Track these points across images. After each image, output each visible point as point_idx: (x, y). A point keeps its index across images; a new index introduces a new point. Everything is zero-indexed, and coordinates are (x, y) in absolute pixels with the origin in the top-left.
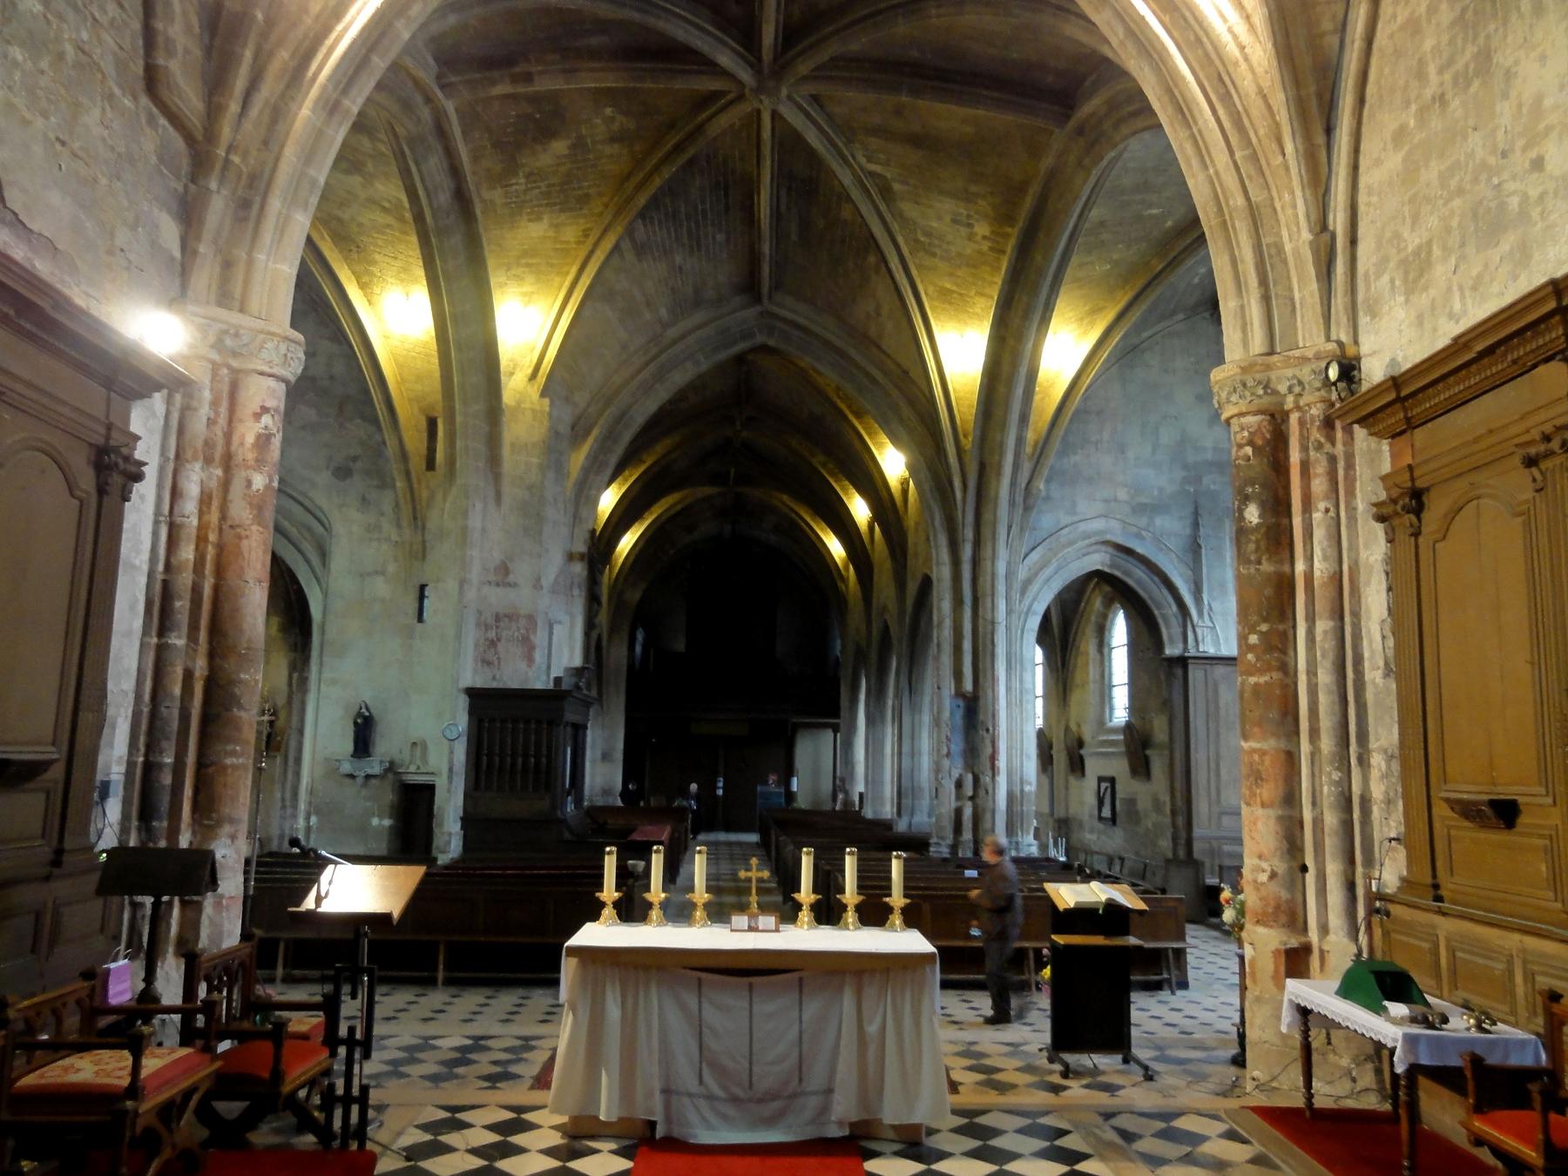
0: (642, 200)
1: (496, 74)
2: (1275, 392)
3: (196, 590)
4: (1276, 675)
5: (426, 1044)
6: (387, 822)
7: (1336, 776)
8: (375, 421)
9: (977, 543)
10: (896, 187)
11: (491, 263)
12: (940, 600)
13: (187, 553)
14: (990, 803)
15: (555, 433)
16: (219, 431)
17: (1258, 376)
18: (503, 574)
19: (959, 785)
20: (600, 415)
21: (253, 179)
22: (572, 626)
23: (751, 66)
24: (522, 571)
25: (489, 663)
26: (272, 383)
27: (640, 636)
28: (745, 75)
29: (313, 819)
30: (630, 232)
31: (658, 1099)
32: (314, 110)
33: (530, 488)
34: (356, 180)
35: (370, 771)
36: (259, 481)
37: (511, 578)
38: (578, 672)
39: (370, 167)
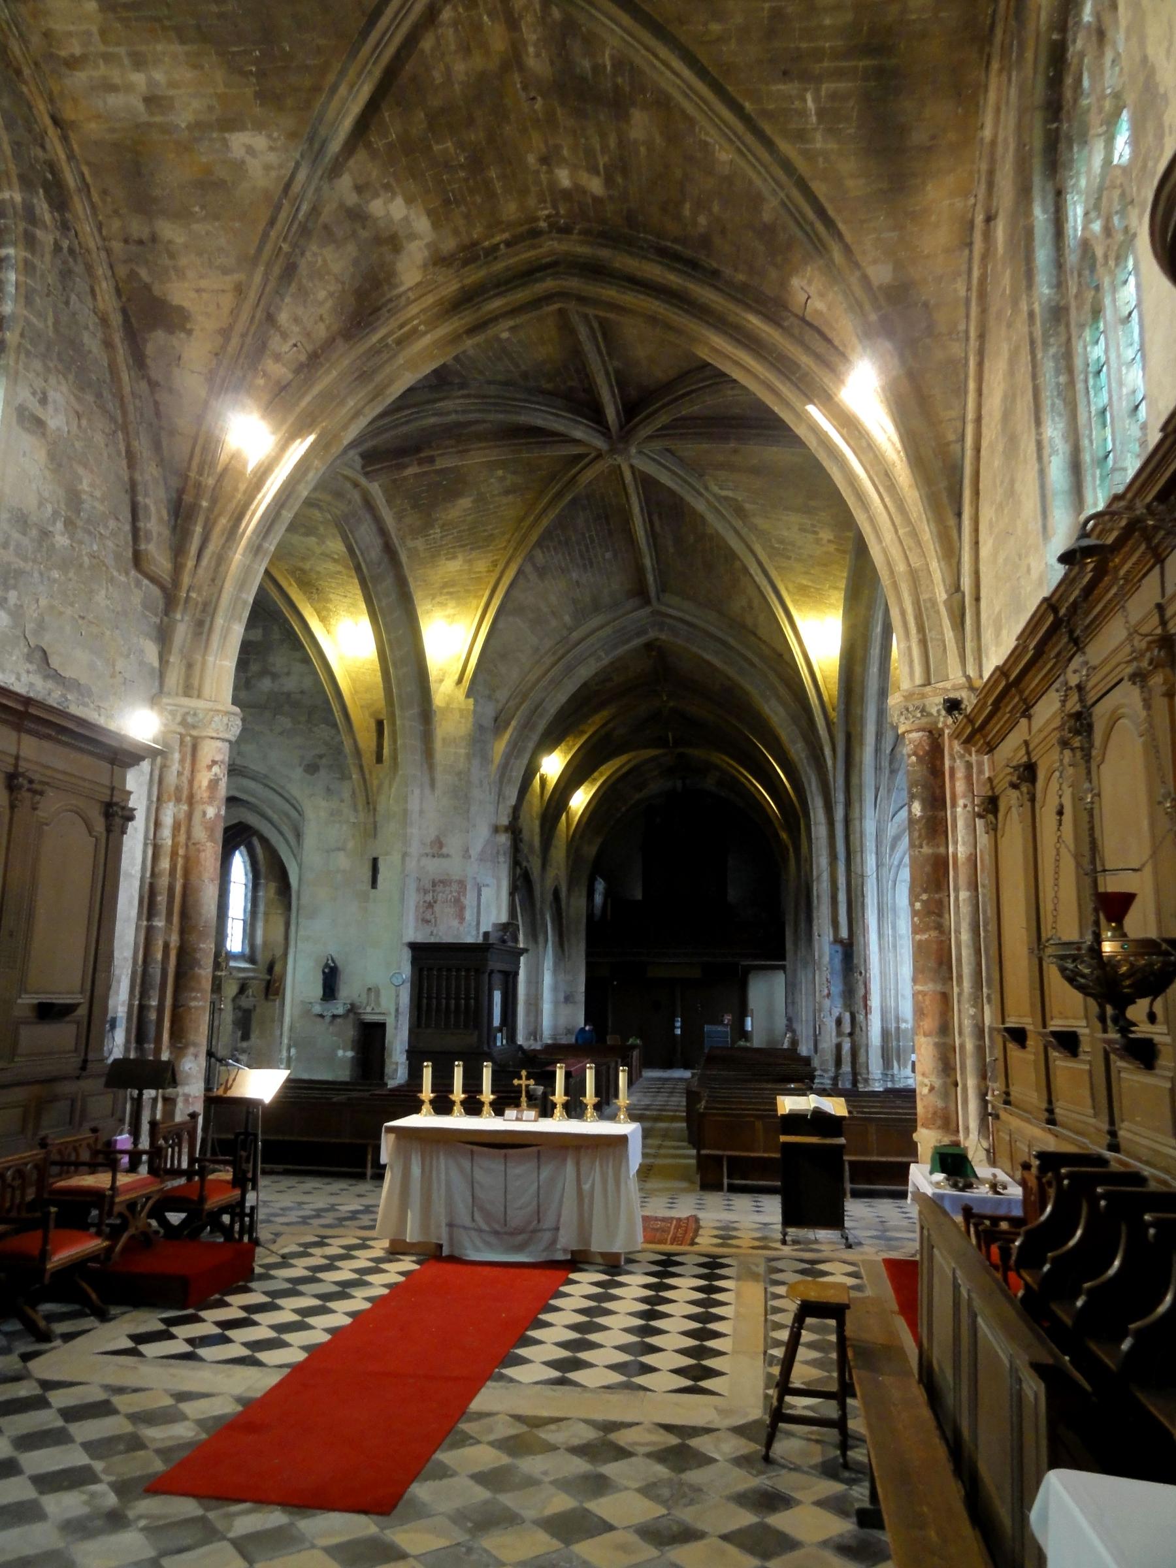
0: (534, 537)
1: (406, 460)
2: (930, 714)
3: (171, 889)
4: (934, 934)
5: (332, 1208)
6: (350, 1054)
7: (972, 1011)
8: (335, 725)
9: (848, 804)
10: (747, 506)
11: (418, 596)
13: (165, 864)
14: (864, 1040)
15: (480, 728)
16: (185, 780)
17: (917, 703)
18: (437, 848)
19: (839, 1022)
20: (517, 709)
21: (206, 605)
22: (499, 887)
23: (603, 434)
24: (453, 844)
25: (428, 922)
26: (219, 744)
27: (600, 886)
28: (600, 443)
29: (293, 1051)
30: (530, 558)
31: (444, 1231)
32: (243, 555)
33: (459, 774)
34: (312, 540)
35: (336, 1012)
36: (211, 812)
37: (445, 850)
38: (504, 927)
39: (322, 529)
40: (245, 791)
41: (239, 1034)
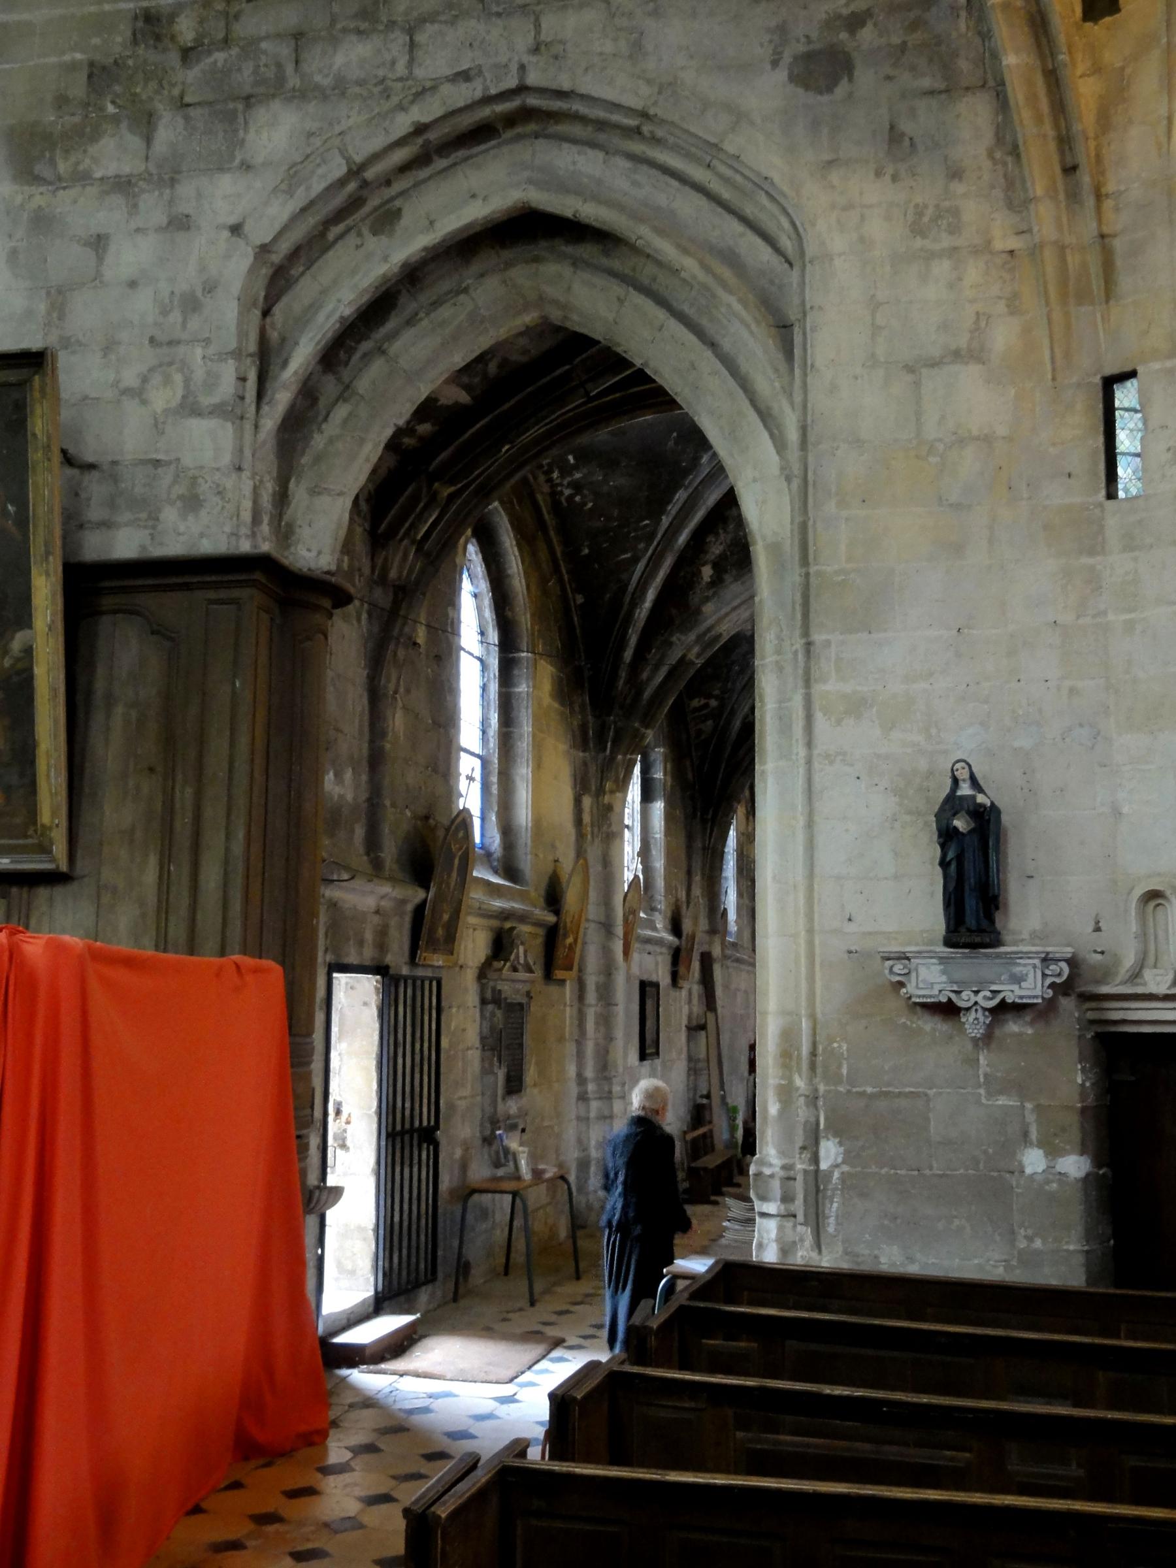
29: (830, 1152)
35: (1012, 993)
40: (563, 187)
41: (501, 1074)
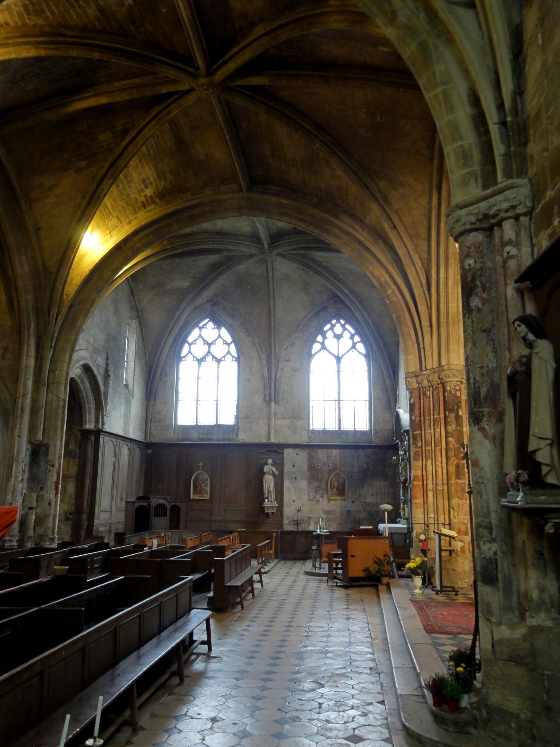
12: (26, 380)
